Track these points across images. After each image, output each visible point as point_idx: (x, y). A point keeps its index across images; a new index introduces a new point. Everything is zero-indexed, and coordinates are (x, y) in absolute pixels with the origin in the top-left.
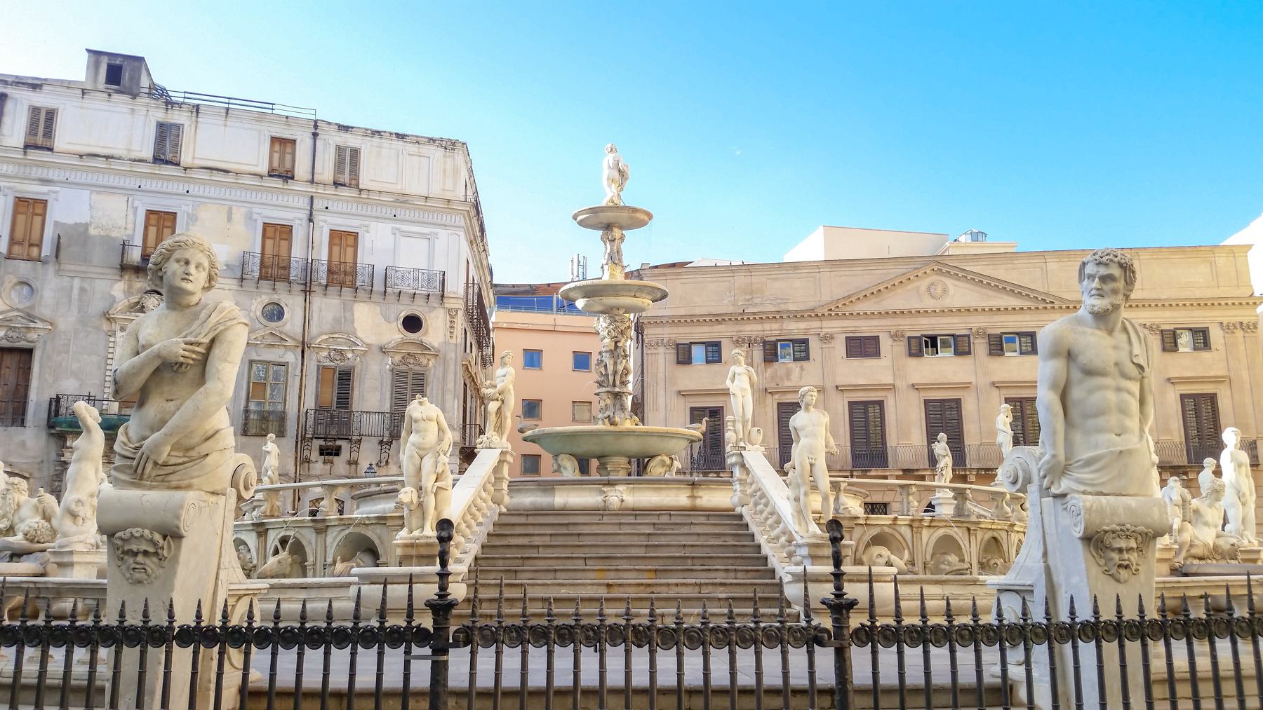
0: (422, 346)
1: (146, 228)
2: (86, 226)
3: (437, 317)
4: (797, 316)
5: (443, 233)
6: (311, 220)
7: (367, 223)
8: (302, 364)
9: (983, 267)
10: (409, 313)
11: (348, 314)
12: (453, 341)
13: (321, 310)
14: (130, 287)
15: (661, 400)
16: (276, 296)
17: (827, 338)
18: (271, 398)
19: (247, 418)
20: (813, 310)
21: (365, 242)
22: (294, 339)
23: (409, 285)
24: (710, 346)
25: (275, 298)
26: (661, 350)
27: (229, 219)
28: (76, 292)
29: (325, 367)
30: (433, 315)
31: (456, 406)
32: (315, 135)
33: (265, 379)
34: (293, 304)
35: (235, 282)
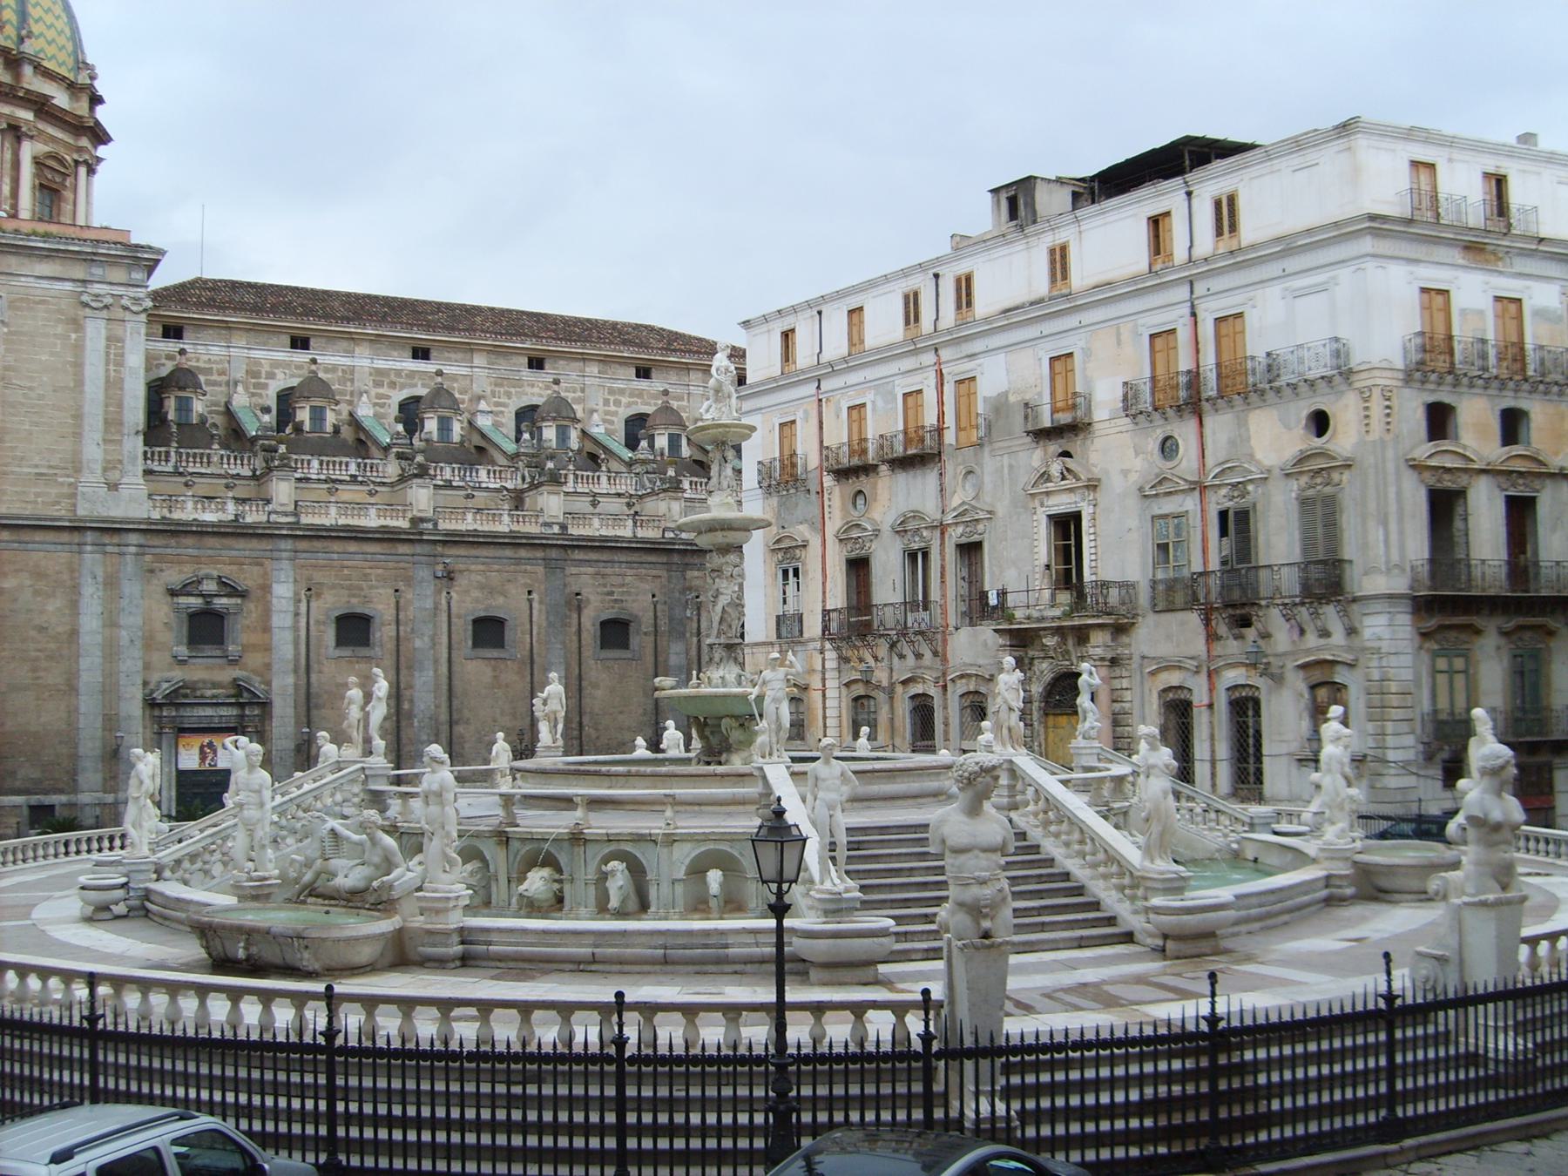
0: (1323, 454)
1: (1052, 380)
2: (1006, 394)
3: (1347, 406)
5: (1344, 274)
6: (1194, 315)
7: (1252, 294)
10: (1313, 408)
12: (1370, 438)
14: (1046, 452)
18: (1175, 561)
21: (1252, 320)
22: (1185, 480)
27: (1119, 343)
28: (1006, 470)
31: (1381, 538)
32: (1189, 194)
34: (1185, 432)
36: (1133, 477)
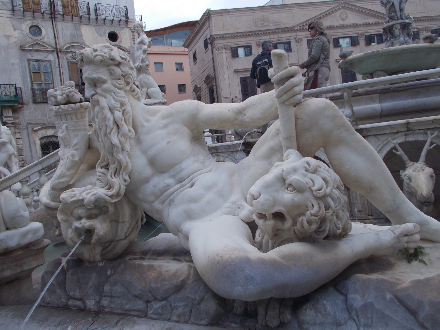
4: (286, 30)
8: (59, 61)
9: (362, 4)
10: (111, 31)
11: (78, 32)
13: (63, 30)
15: (226, 75)
16: (35, 21)
17: (299, 41)
18: (46, 81)
19: (34, 93)
20: (293, 27)
23: (110, 14)
24: (246, 47)
25: (35, 22)
26: (224, 51)
29: (72, 63)
30: (123, 31)
33: (39, 70)
35: (9, 12)
36: (13, 40)
